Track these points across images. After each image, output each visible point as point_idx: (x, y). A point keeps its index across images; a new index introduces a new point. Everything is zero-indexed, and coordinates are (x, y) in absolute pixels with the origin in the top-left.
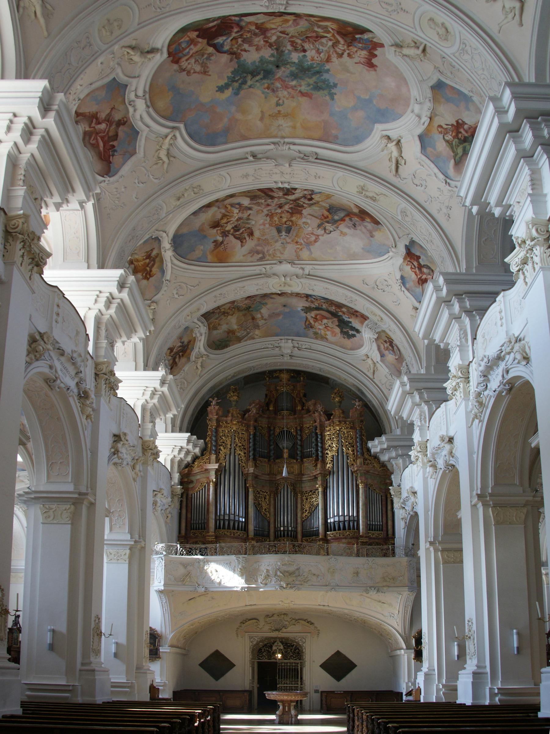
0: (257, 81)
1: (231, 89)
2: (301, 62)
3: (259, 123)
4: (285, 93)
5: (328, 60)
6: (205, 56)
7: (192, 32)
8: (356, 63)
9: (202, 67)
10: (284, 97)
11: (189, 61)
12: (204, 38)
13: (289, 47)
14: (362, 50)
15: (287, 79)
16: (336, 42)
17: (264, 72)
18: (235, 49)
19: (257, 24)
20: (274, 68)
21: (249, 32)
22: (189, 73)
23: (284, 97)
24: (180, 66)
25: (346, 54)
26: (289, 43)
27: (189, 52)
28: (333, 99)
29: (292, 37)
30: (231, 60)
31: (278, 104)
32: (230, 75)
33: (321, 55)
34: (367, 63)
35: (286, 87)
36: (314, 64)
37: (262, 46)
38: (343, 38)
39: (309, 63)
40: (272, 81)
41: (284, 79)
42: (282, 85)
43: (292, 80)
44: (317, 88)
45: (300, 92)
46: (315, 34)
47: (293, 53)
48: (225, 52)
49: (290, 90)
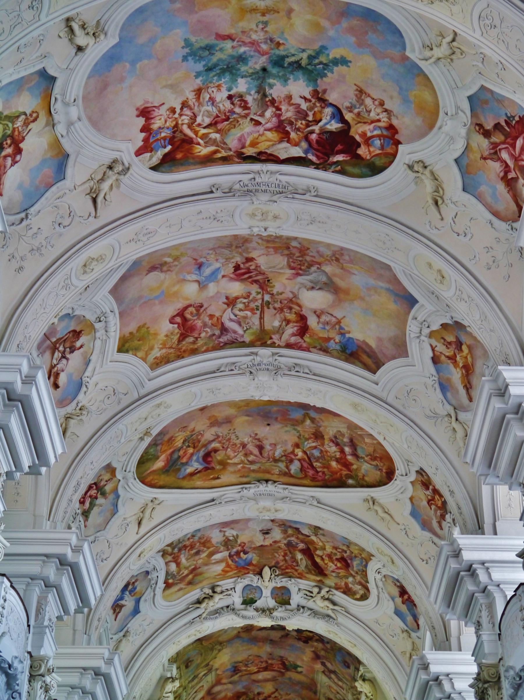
0: (293, 55)
1: (331, 57)
2: (234, 80)
3: (295, 6)
4: (254, 37)
5: (198, 92)
6: (356, 111)
7: (364, 157)
8: (163, 104)
9: (363, 100)
10: (256, 31)
11: (378, 117)
12: (353, 138)
13: (249, 99)
14: (160, 128)
15: (252, 53)
16: (192, 124)
17: (284, 65)
18: (318, 105)
19: (288, 142)
20: (270, 68)
21: (298, 129)
22: (382, 104)
23: (256, 31)
24: (390, 119)
25: (178, 111)
26: (249, 105)
27: (375, 129)
28: (185, 40)
29: (246, 116)
30: (325, 91)
31: (266, 23)
32: (329, 74)
33: (209, 96)
34: (149, 112)
35: (253, 43)
36: (217, 81)
37: (283, 103)
38: (185, 135)
39: (223, 80)
40: (273, 52)
41: (256, 54)
42: (259, 46)
43: (245, 52)
44: (209, 48)
45: (233, 40)
46: (219, 128)
47: (245, 90)
48: (331, 105)
49: (248, 40)
